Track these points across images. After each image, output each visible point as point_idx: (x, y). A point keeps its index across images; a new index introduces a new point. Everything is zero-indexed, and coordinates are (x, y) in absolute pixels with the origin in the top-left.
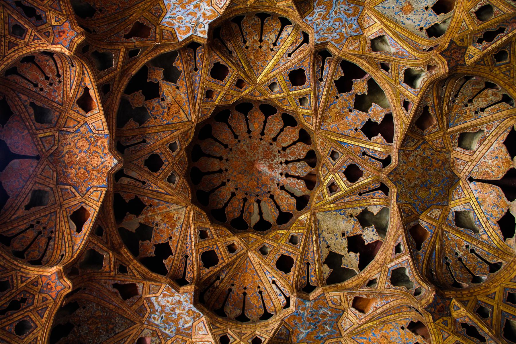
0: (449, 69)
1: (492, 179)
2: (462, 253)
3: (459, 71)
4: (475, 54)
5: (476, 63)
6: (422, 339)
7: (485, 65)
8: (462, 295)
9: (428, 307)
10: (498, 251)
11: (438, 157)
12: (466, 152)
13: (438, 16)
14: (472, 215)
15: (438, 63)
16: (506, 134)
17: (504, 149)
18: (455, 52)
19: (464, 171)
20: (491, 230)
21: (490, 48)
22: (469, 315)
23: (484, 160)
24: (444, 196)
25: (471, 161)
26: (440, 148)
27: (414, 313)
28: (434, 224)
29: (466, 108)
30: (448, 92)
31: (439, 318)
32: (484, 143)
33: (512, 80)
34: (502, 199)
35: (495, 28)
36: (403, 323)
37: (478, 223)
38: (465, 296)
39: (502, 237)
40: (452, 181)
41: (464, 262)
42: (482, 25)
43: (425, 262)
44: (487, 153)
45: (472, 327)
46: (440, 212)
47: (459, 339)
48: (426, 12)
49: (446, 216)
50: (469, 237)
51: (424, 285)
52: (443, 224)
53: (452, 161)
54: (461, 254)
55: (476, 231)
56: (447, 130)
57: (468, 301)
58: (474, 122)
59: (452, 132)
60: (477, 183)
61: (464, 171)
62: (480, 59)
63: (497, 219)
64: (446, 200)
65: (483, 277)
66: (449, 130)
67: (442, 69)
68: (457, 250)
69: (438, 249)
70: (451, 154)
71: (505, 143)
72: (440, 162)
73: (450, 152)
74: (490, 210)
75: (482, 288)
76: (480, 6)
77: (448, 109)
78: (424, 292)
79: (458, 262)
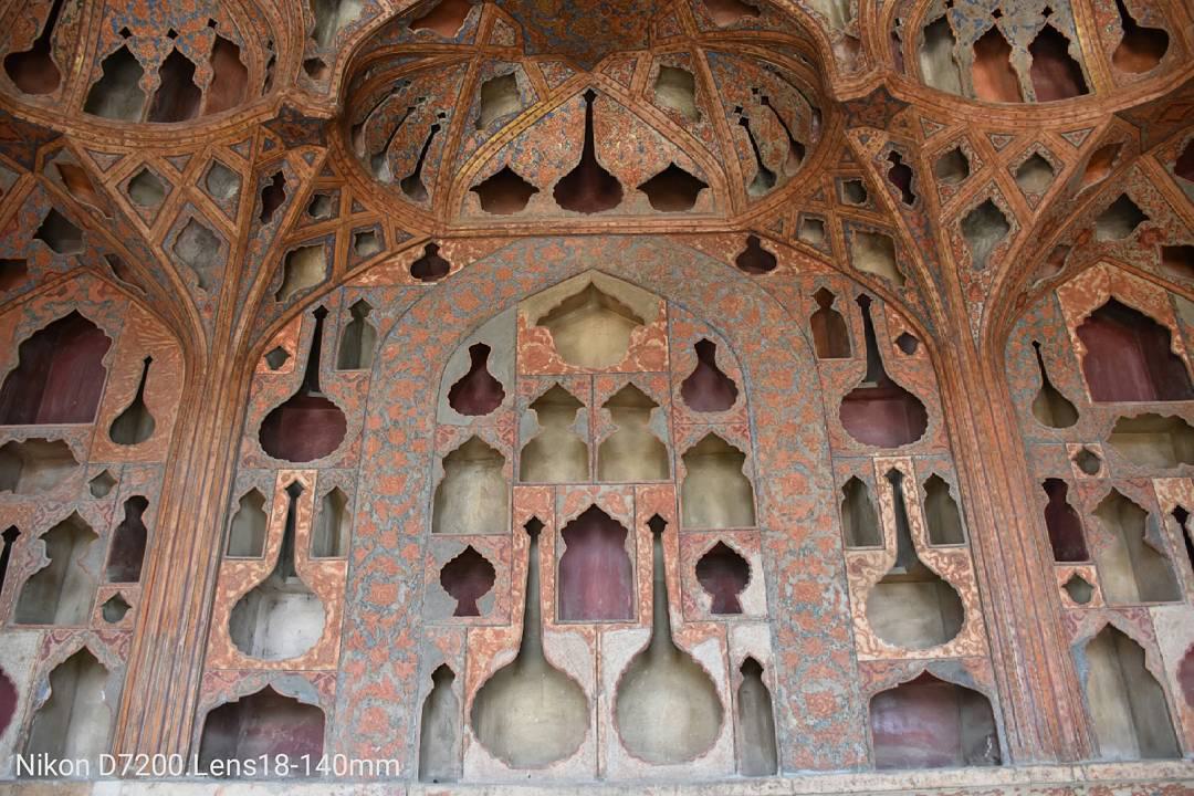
0: (843, 103)
1: (595, 142)
2: (426, 111)
3: (835, 116)
4: (868, 146)
5: (848, 149)
6: (208, 81)
7: (842, 161)
8: (342, 159)
9: (290, 111)
10: (448, 179)
11: (638, 26)
12: (649, 85)
13: (970, 46)
14: (512, 106)
15: (859, 78)
16: (690, 169)
17: (661, 166)
18: (879, 112)
19: (607, 80)
20: (488, 155)
21: (876, 176)
22: (305, 186)
23: (634, 123)
24: (546, 45)
25: (631, 95)
26: (658, 28)
27: (261, 56)
28: (478, 40)
29: (749, 89)
30: (789, 62)
31: (275, 132)
32: (672, 124)
33: (804, 201)
34: (557, 171)
35: (915, 188)
36: (225, 24)
37: (498, 125)
38: (340, 164)
39: (478, 181)
40: (581, 57)
41: (407, 120)
42: (927, 166)
43: (388, 50)
44: (650, 128)
45: (282, 195)
46: (507, 44)
47: (247, 179)
48: (990, 12)
49: (502, 58)
50: (465, 114)
51: (338, 80)
52: (483, 57)
53: (630, 53)
54: (424, 107)
55: (478, 125)
56: (702, 47)
57: (333, 175)
58: (718, 104)
59: (697, 58)
60: (583, 111)
61: (608, 81)
62: (857, 155)
63: (513, 166)
64: (537, 50)
65: (386, 165)
66: (700, 51)
67: (845, 85)
68: (430, 99)
69: (425, 64)
70: (645, 52)
71: (673, 171)
72: (624, 32)
73: (649, 49)
74: (530, 147)
75: (367, 186)
76: (970, 158)
77: (749, 55)
78: (320, 89)
79: (406, 109)
